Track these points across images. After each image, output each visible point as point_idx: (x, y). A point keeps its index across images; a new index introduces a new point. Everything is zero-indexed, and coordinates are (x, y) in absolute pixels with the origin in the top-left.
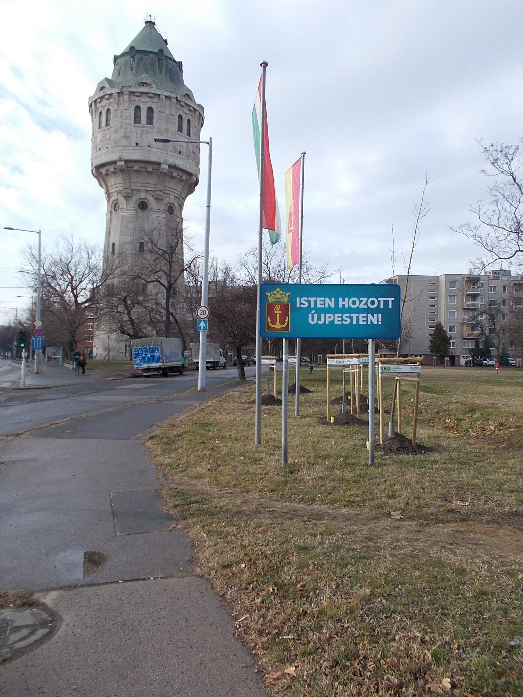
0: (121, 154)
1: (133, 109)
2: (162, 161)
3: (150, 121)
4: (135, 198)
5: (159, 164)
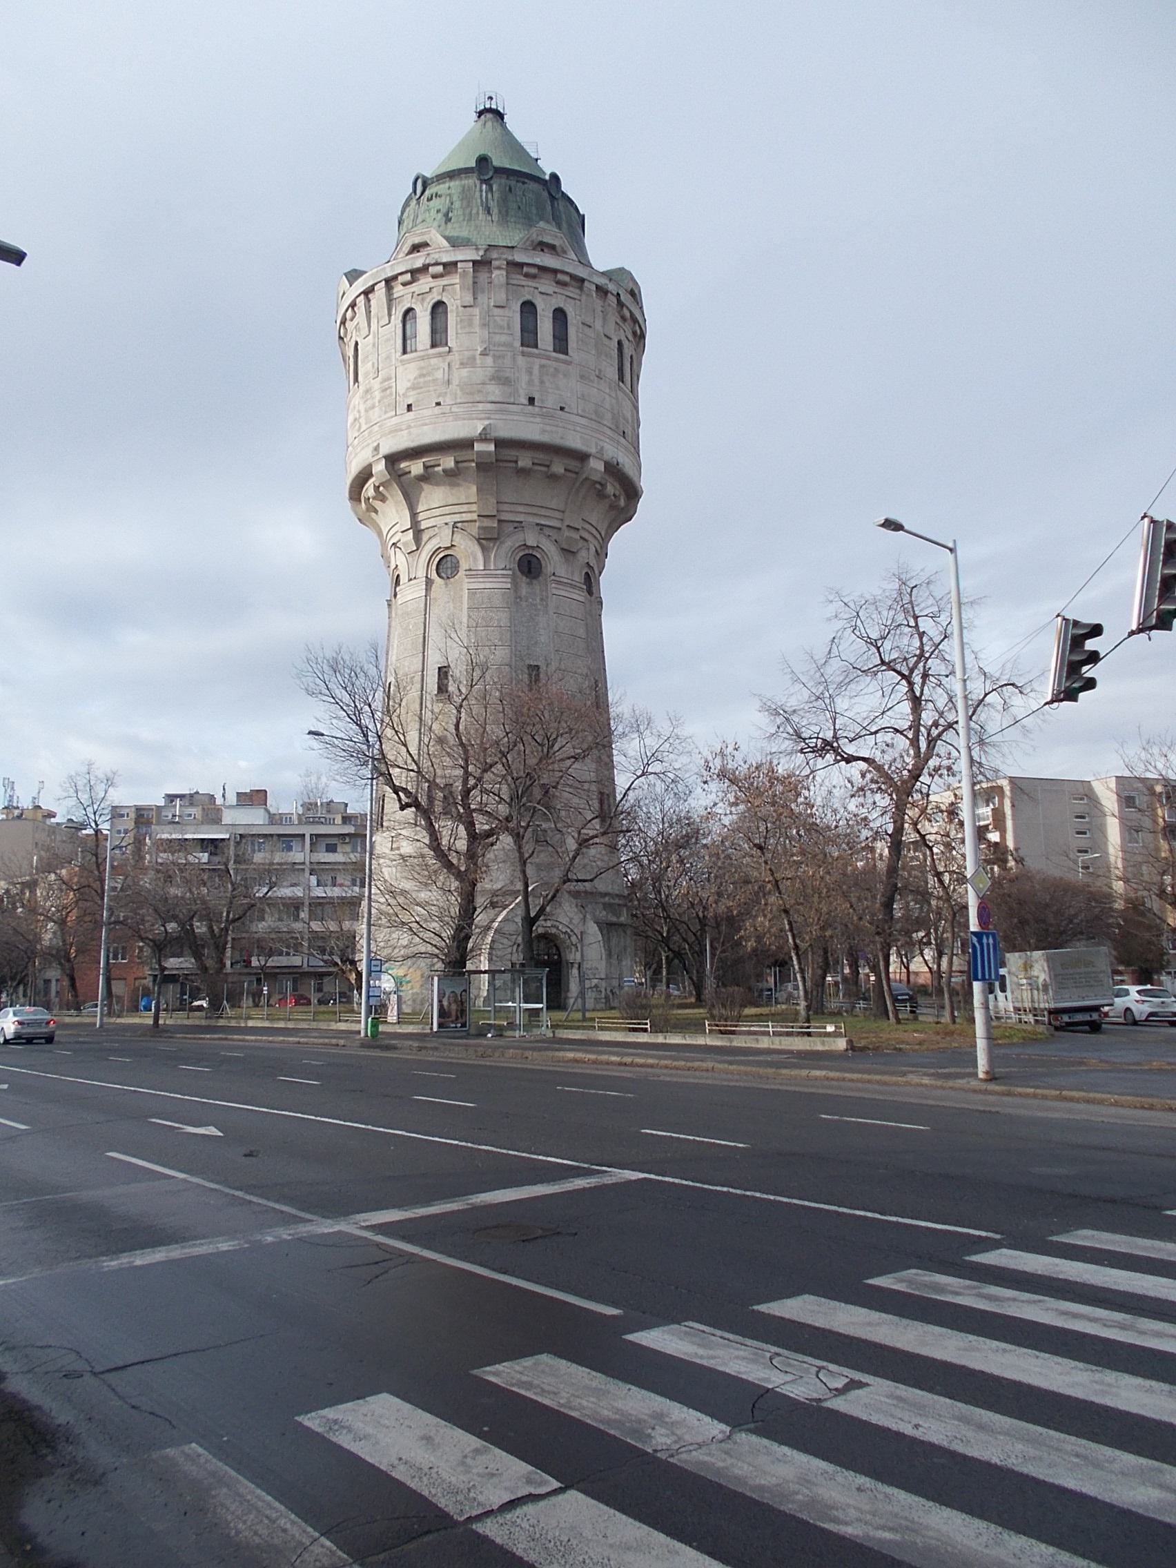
0: (486, 422)
1: (517, 307)
2: (593, 450)
3: (561, 343)
4: (509, 544)
5: (583, 457)
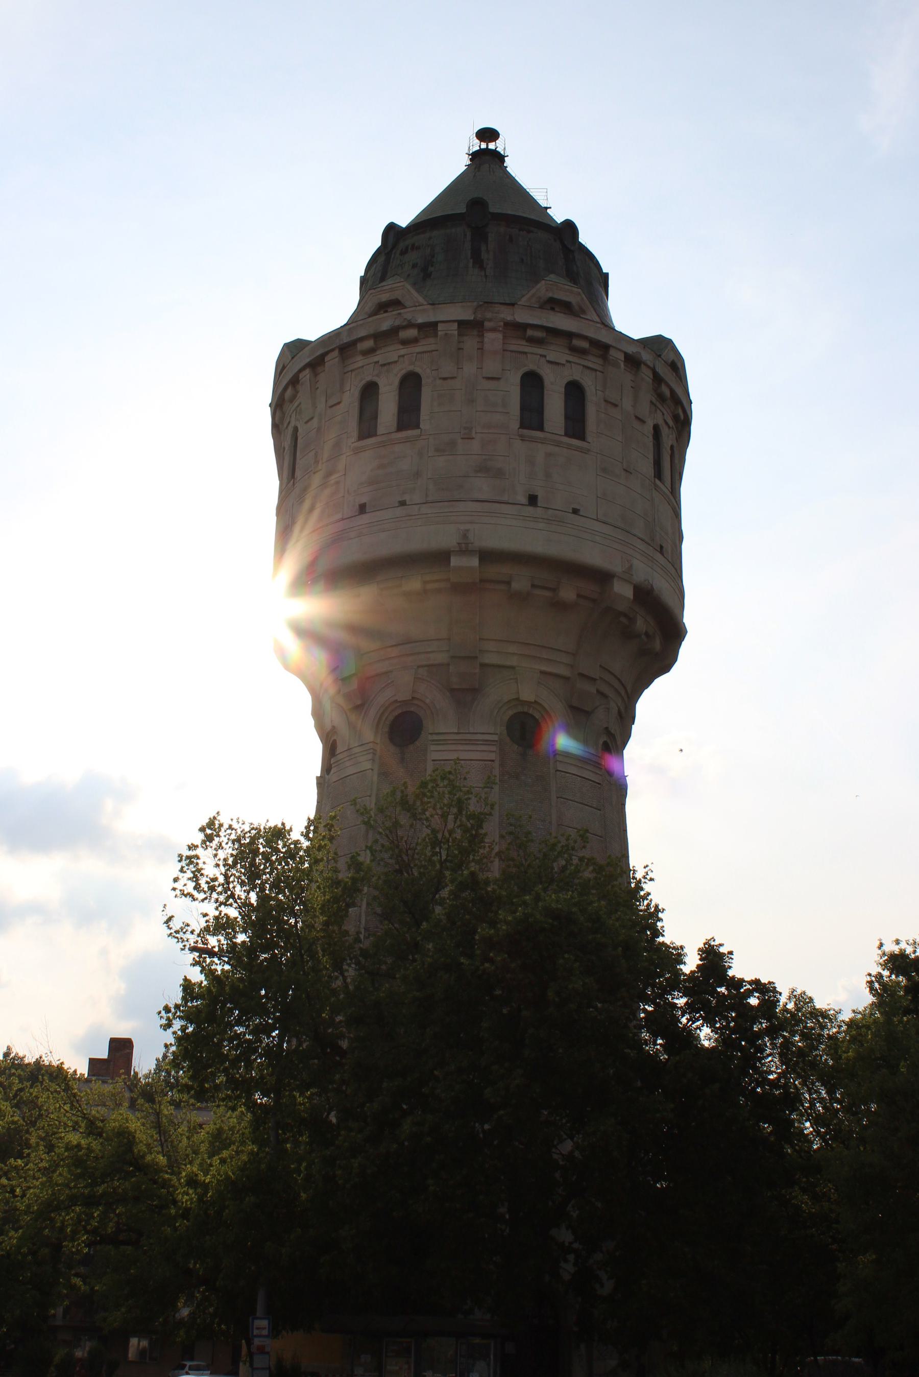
1: (514, 379)
3: (576, 425)
5: (603, 577)
